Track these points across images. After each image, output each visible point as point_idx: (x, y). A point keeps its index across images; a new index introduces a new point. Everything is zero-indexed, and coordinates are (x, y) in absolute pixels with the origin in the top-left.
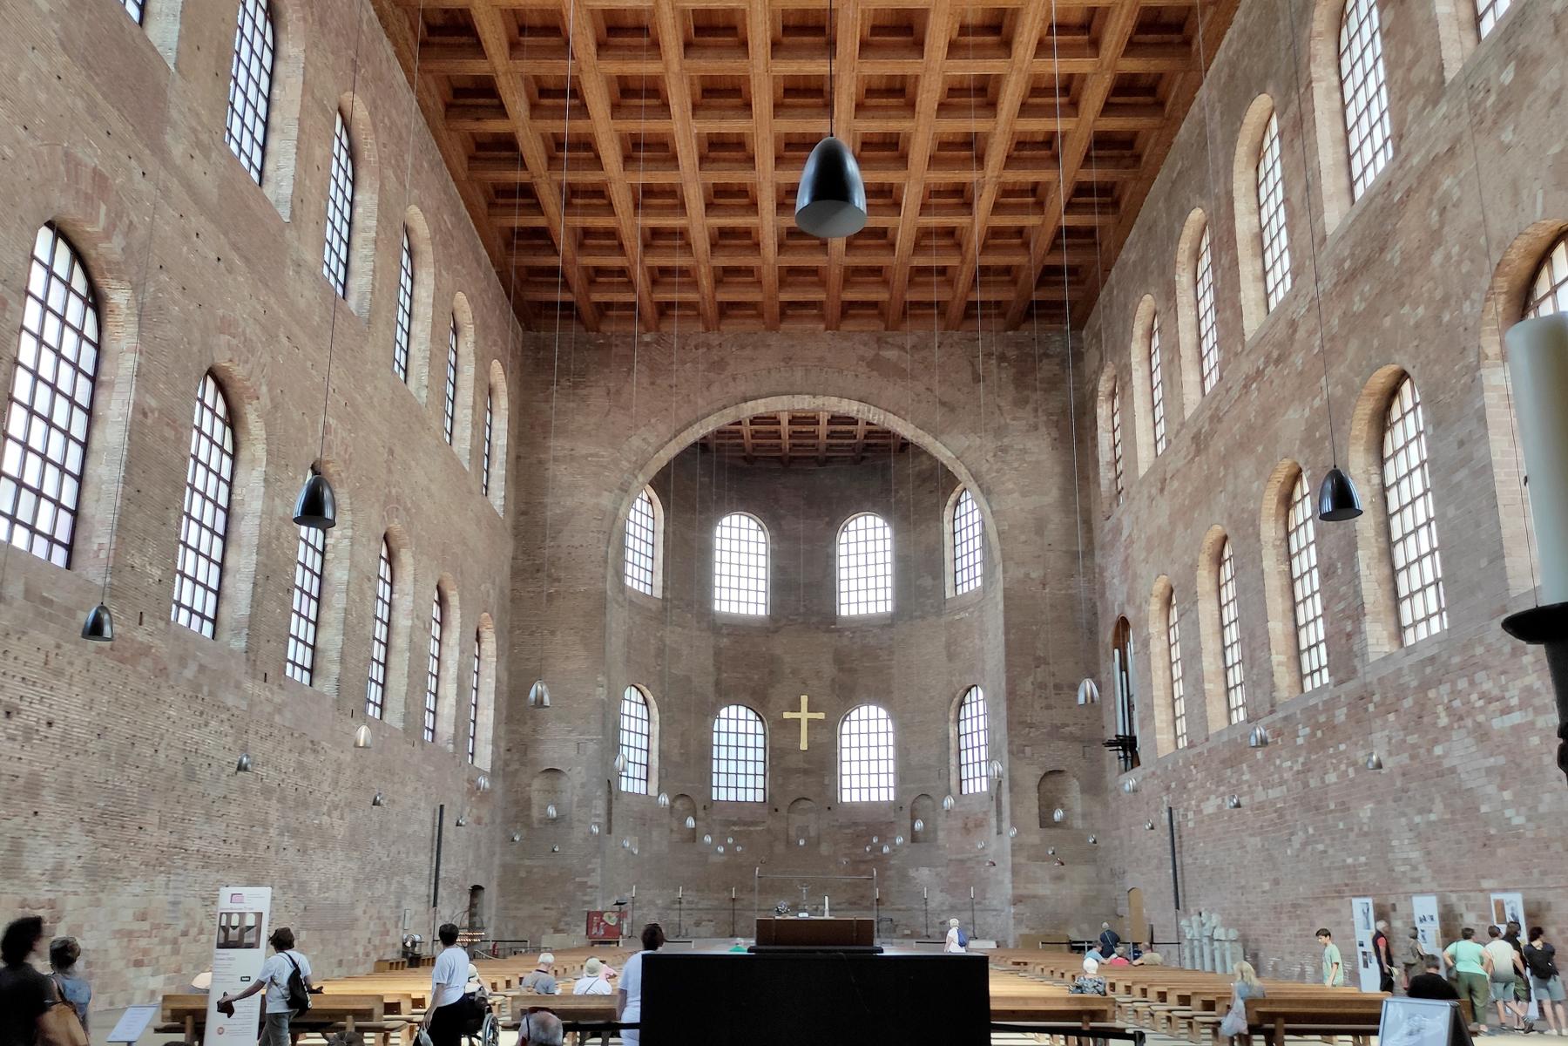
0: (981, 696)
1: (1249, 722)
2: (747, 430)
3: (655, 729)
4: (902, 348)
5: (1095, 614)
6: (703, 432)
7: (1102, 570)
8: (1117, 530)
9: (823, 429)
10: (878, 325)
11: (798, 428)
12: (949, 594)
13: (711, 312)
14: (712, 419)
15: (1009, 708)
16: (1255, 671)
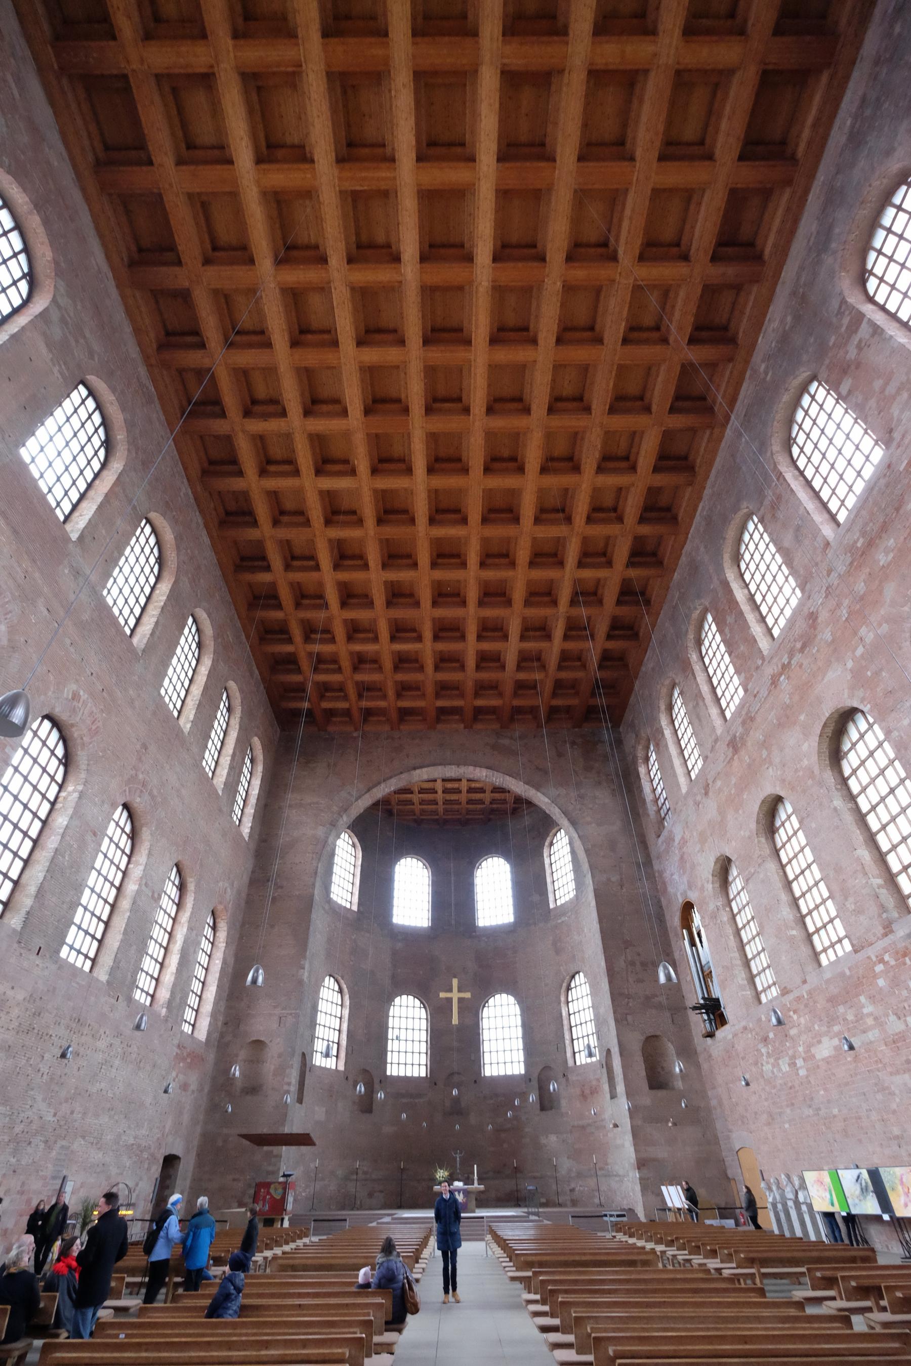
0: (583, 981)
1: (856, 951)
2: (416, 798)
3: (346, 1012)
4: (511, 738)
5: (661, 907)
6: (387, 790)
7: (661, 873)
8: (671, 839)
9: (463, 797)
10: (496, 726)
11: (449, 797)
12: (552, 906)
13: (394, 715)
14: (393, 781)
15: (610, 982)
16: (851, 899)
